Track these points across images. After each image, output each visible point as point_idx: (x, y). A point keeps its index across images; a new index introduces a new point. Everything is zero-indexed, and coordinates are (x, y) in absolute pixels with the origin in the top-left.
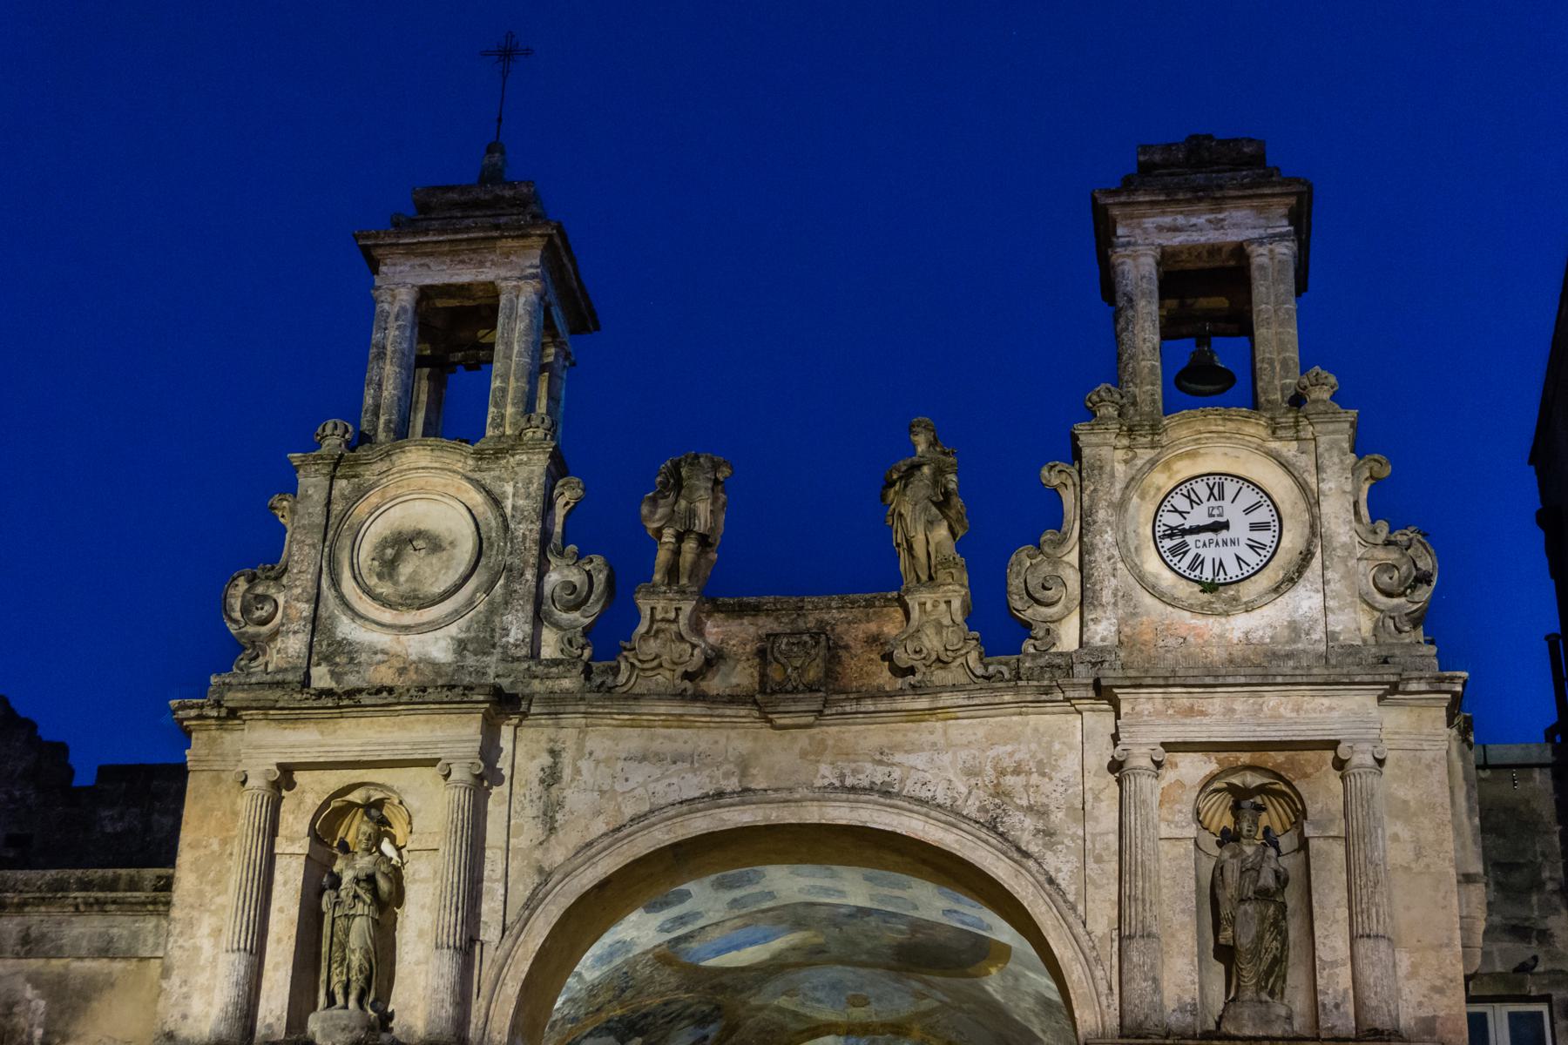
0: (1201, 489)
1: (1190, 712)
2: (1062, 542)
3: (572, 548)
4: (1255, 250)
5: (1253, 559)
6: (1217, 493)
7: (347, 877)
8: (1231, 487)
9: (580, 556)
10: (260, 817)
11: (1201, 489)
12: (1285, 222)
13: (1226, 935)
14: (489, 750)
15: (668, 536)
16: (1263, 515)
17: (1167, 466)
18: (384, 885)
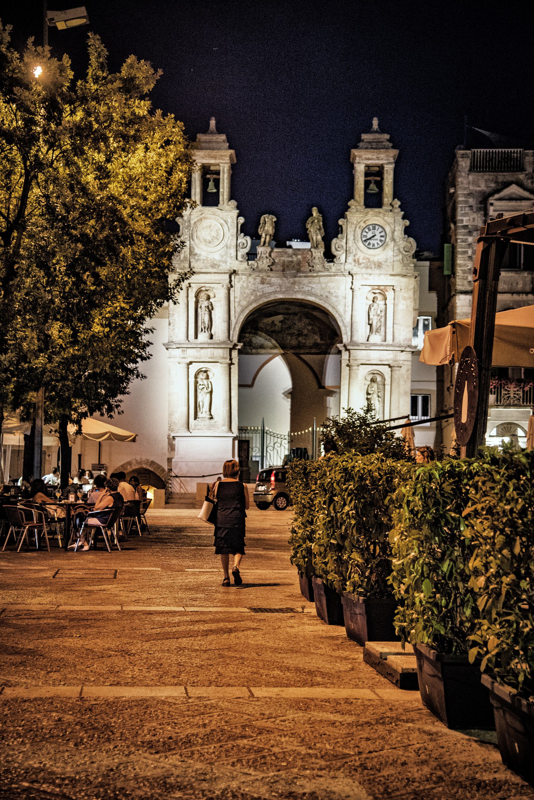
0: (371, 227)
1: (366, 279)
2: (342, 238)
3: (242, 234)
4: (385, 166)
5: (380, 244)
6: (374, 228)
7: (203, 306)
8: (377, 227)
9: (245, 236)
10: (185, 295)
11: (371, 227)
12: (392, 159)
13: (370, 322)
14: (230, 281)
15: (264, 235)
16: (383, 234)
17: (365, 222)
18: (210, 307)
